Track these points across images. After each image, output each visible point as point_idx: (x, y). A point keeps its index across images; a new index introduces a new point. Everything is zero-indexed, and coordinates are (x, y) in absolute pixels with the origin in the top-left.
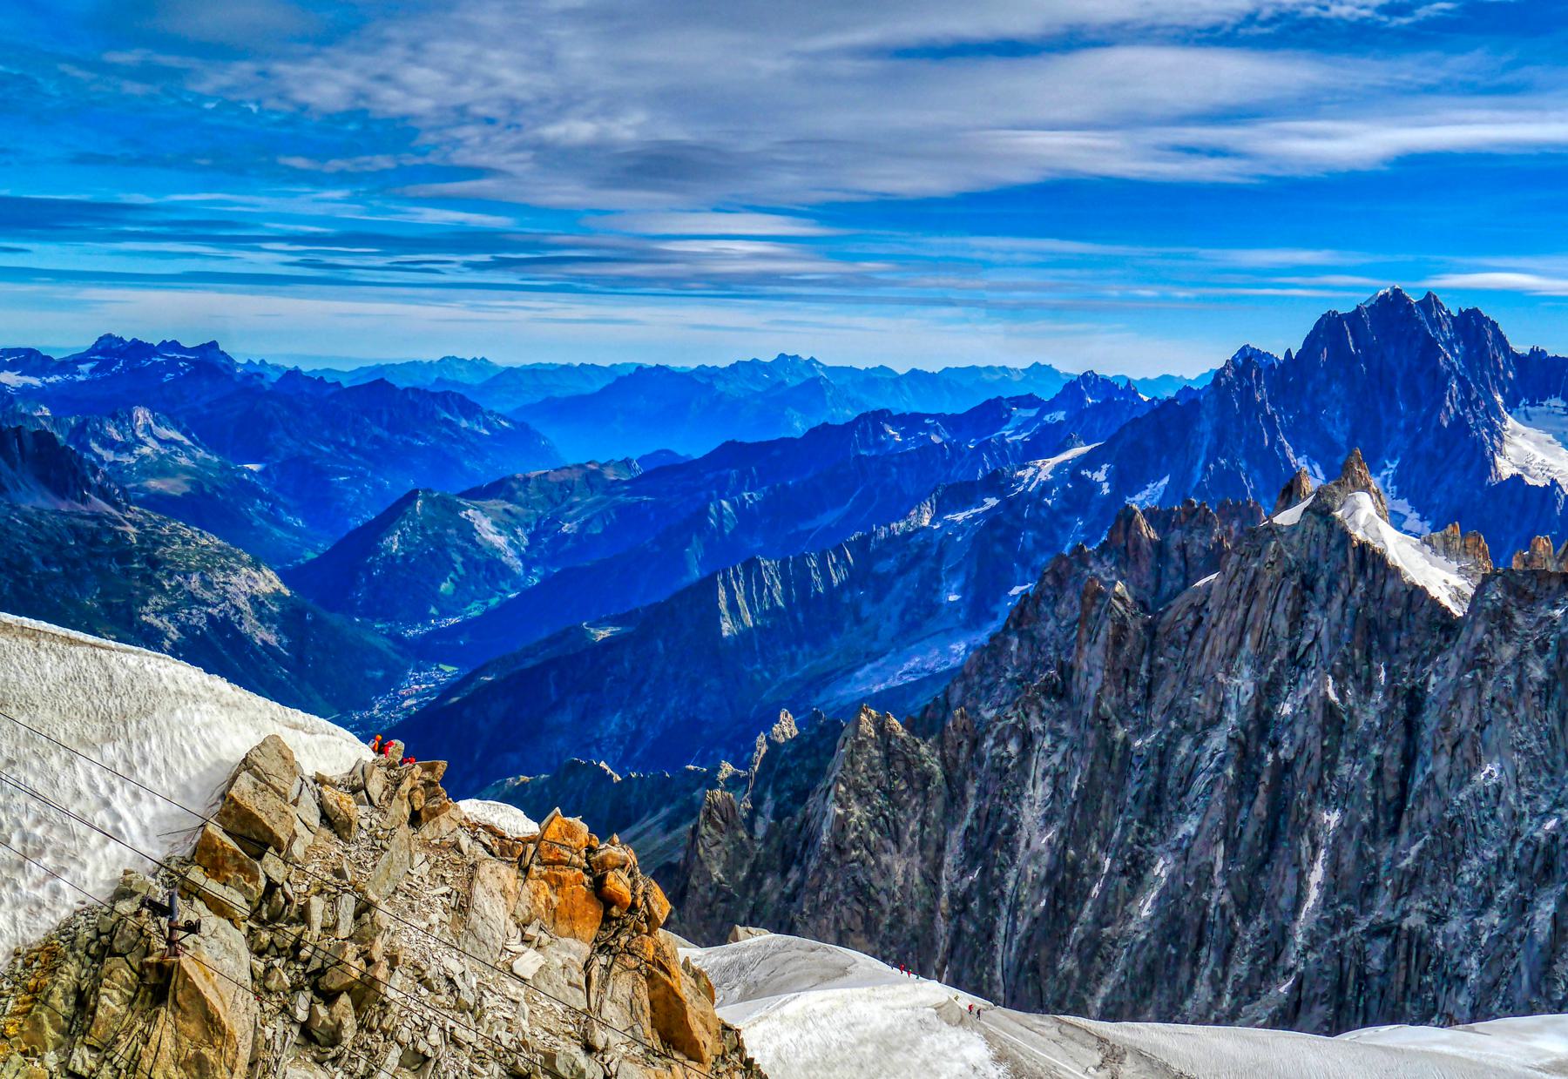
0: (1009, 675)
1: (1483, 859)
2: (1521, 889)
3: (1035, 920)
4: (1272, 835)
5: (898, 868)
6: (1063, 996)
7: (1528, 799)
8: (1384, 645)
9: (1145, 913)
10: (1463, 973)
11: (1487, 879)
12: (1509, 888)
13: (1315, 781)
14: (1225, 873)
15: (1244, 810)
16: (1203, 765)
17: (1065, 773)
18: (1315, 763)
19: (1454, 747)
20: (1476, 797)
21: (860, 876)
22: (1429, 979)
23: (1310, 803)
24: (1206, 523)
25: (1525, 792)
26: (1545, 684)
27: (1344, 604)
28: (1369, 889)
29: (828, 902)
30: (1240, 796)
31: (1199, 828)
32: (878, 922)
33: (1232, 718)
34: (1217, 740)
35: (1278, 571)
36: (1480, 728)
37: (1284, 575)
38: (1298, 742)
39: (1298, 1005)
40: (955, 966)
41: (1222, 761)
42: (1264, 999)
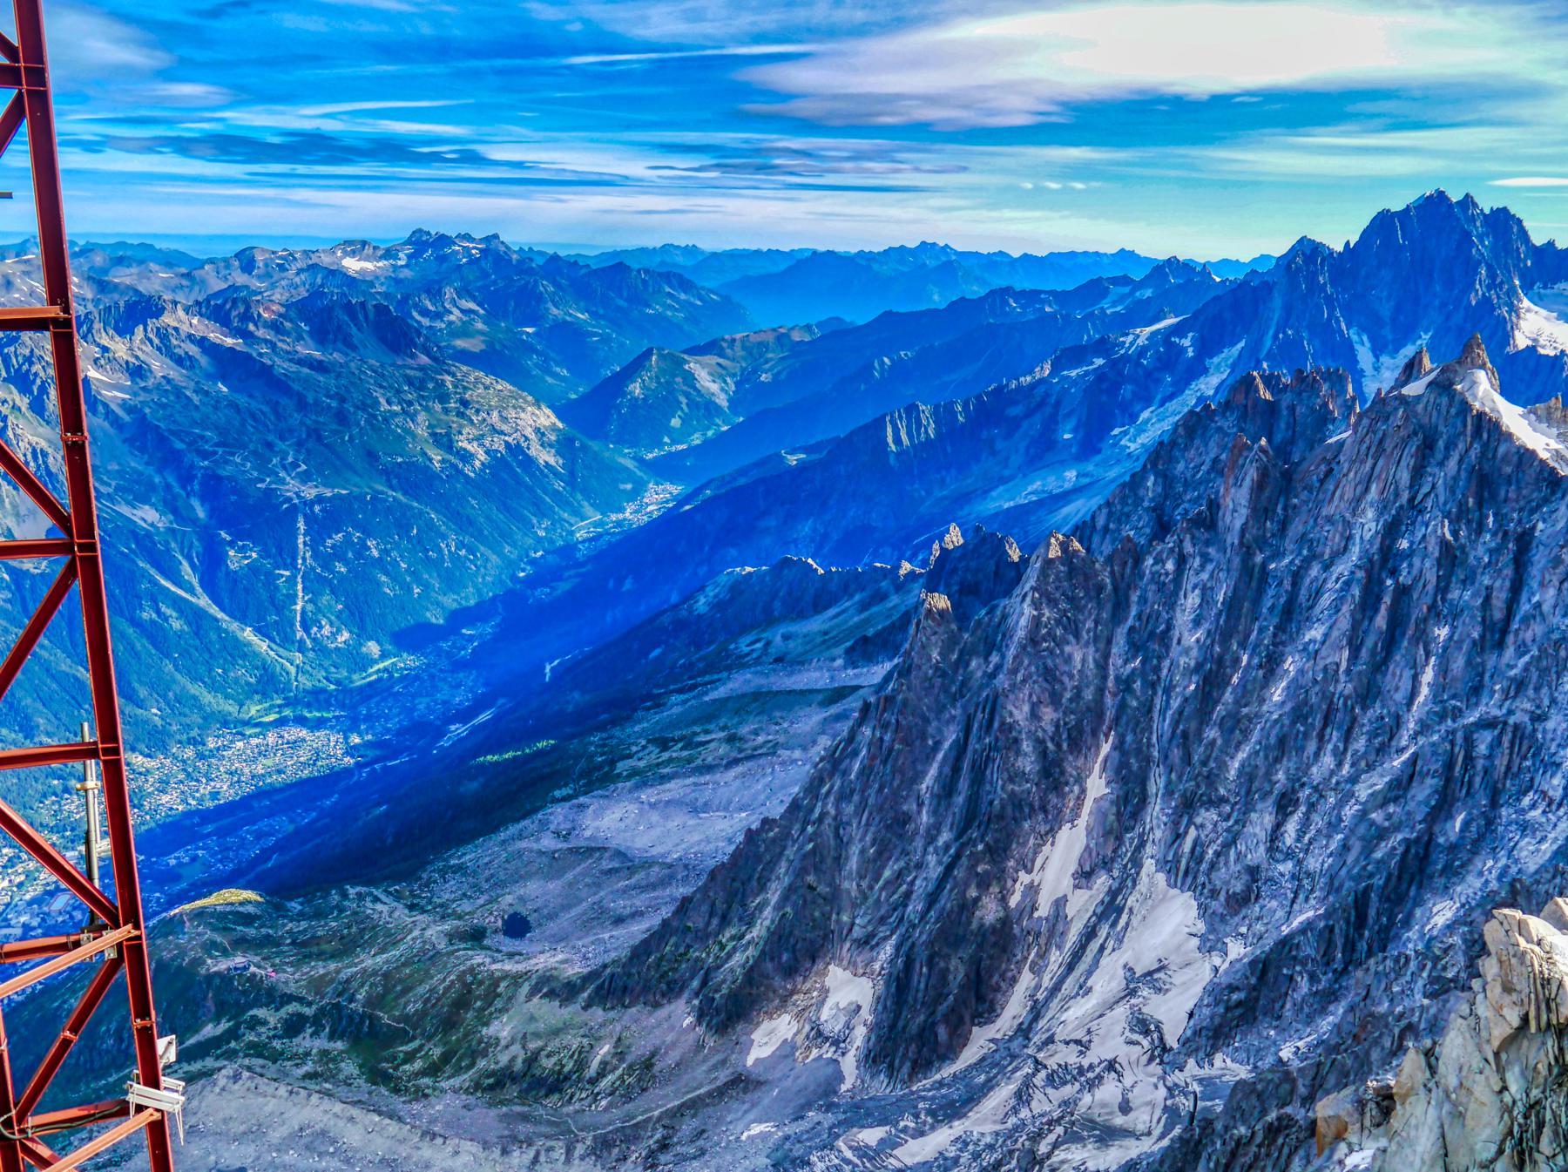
0: (1146, 504)
3: (1186, 700)
4: (1390, 641)
5: (1078, 657)
6: (1208, 758)
8: (1494, 496)
9: (1276, 698)
10: (1558, 760)
13: (1428, 600)
14: (1348, 671)
16: (1329, 586)
17: (1212, 589)
18: (1430, 588)
19: (1561, 583)
21: (1049, 662)
24: (1313, 386)
27: (1460, 462)
28: (1476, 691)
29: (1024, 681)
30: (1364, 611)
31: (1326, 635)
32: (1062, 696)
35: (1403, 433)
38: (1415, 571)
39: (1411, 777)
40: (1120, 730)
41: (1348, 584)
42: (1379, 769)
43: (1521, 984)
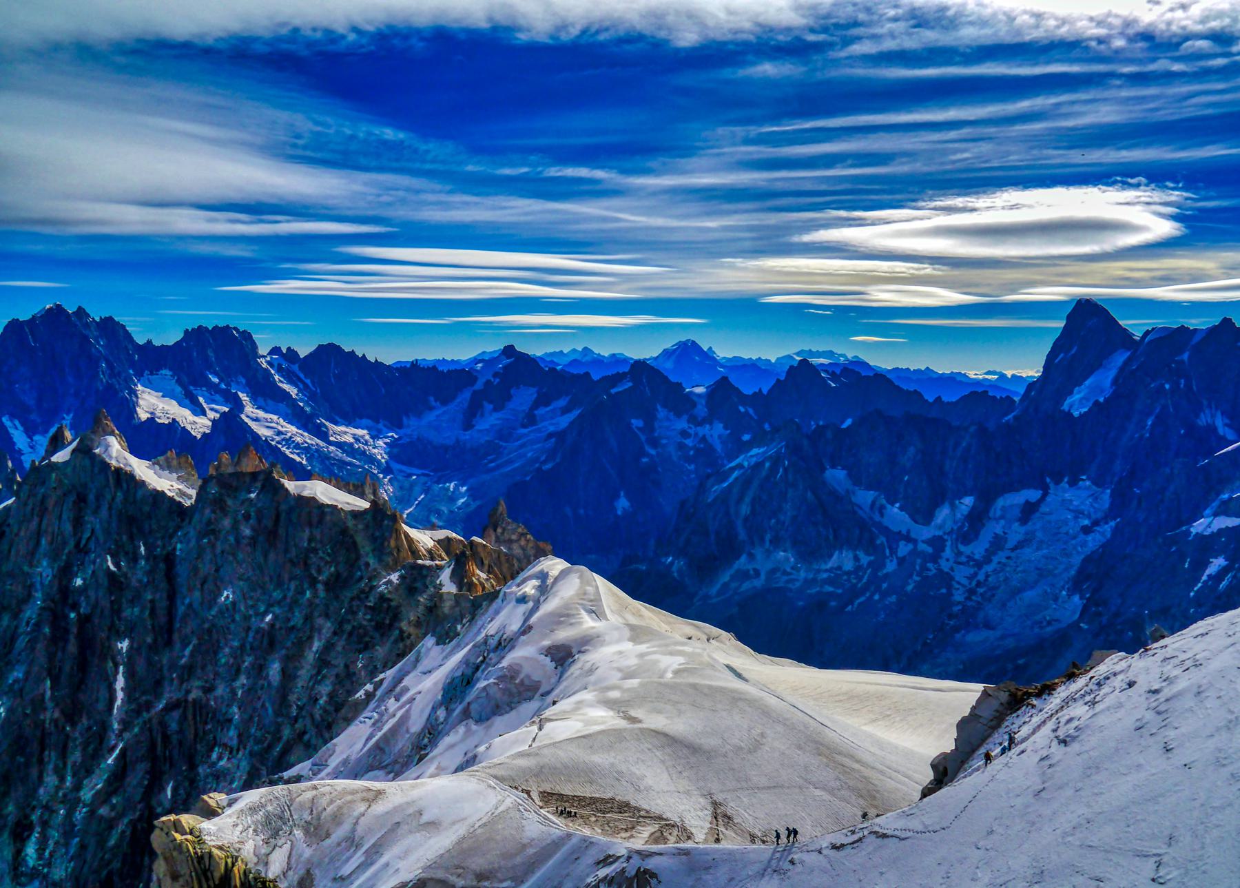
1: (231, 647)
2: (256, 659)
4: (83, 665)
7: (252, 606)
11: (235, 658)
12: (248, 661)
14: (53, 698)
15: (59, 654)
16: (21, 630)
18: (107, 612)
19: (202, 585)
20: (220, 612)
22: (209, 727)
23: (108, 638)
25: (250, 603)
26: (252, 538)
27: (110, 508)
28: (158, 683)
31: (27, 674)
33: (39, 595)
34: (30, 613)
35: (59, 492)
36: (217, 570)
37: (65, 495)
41: (38, 626)
42: (97, 771)
43: (184, 870)
